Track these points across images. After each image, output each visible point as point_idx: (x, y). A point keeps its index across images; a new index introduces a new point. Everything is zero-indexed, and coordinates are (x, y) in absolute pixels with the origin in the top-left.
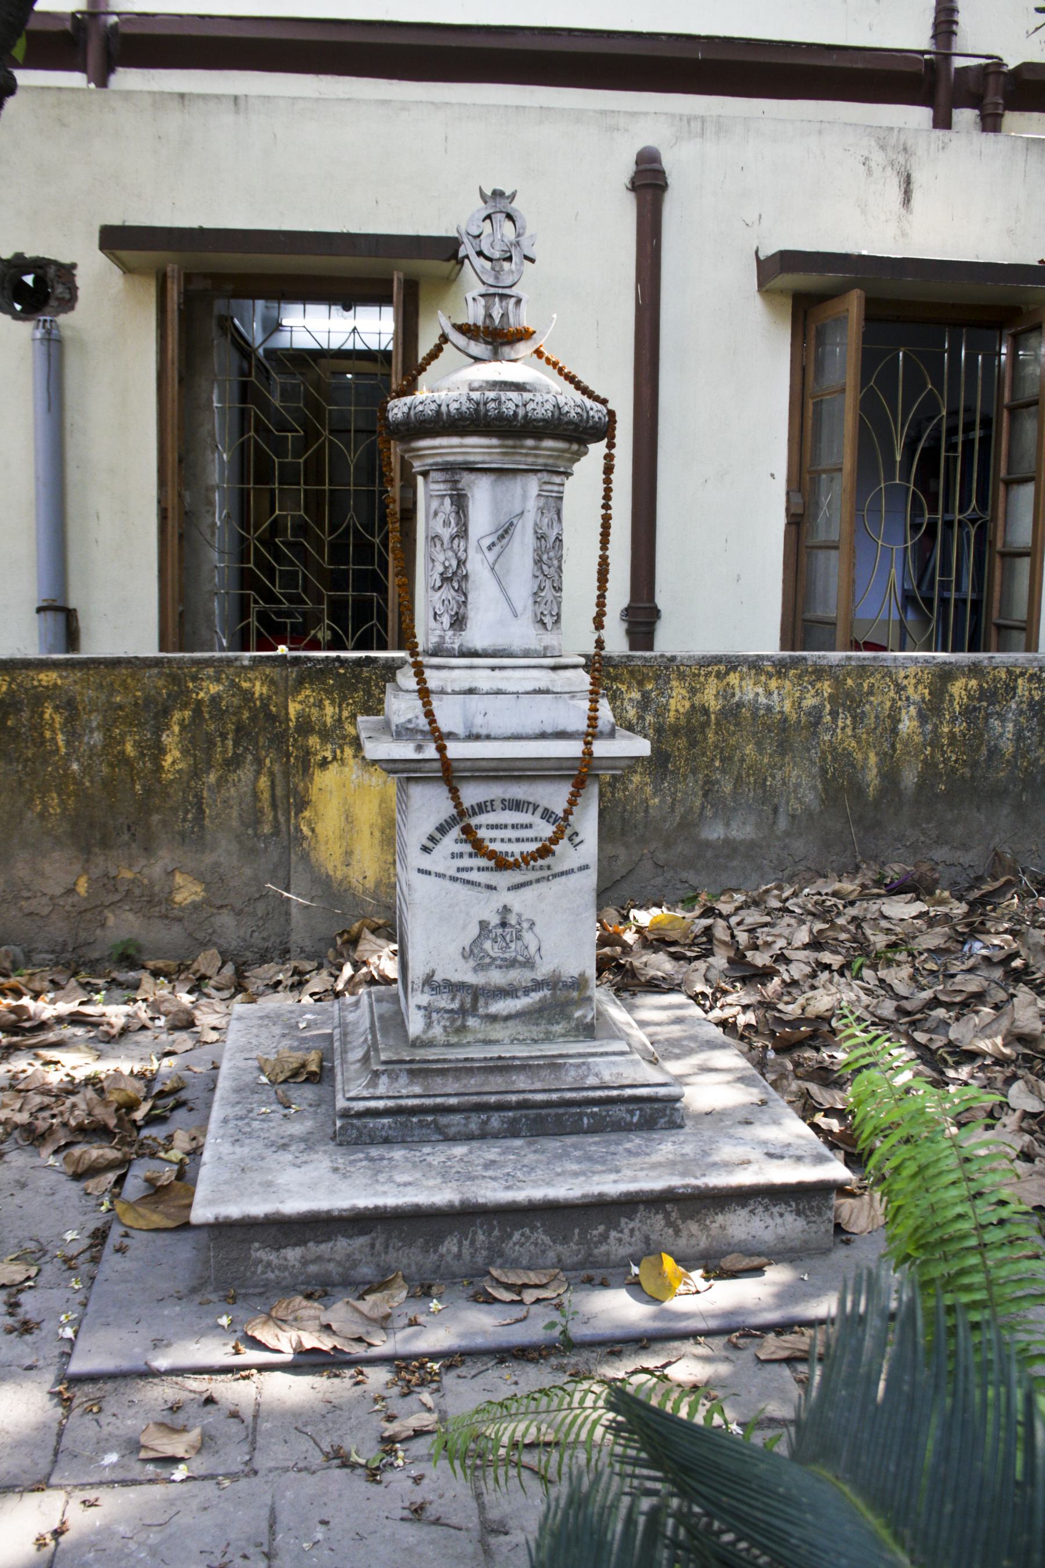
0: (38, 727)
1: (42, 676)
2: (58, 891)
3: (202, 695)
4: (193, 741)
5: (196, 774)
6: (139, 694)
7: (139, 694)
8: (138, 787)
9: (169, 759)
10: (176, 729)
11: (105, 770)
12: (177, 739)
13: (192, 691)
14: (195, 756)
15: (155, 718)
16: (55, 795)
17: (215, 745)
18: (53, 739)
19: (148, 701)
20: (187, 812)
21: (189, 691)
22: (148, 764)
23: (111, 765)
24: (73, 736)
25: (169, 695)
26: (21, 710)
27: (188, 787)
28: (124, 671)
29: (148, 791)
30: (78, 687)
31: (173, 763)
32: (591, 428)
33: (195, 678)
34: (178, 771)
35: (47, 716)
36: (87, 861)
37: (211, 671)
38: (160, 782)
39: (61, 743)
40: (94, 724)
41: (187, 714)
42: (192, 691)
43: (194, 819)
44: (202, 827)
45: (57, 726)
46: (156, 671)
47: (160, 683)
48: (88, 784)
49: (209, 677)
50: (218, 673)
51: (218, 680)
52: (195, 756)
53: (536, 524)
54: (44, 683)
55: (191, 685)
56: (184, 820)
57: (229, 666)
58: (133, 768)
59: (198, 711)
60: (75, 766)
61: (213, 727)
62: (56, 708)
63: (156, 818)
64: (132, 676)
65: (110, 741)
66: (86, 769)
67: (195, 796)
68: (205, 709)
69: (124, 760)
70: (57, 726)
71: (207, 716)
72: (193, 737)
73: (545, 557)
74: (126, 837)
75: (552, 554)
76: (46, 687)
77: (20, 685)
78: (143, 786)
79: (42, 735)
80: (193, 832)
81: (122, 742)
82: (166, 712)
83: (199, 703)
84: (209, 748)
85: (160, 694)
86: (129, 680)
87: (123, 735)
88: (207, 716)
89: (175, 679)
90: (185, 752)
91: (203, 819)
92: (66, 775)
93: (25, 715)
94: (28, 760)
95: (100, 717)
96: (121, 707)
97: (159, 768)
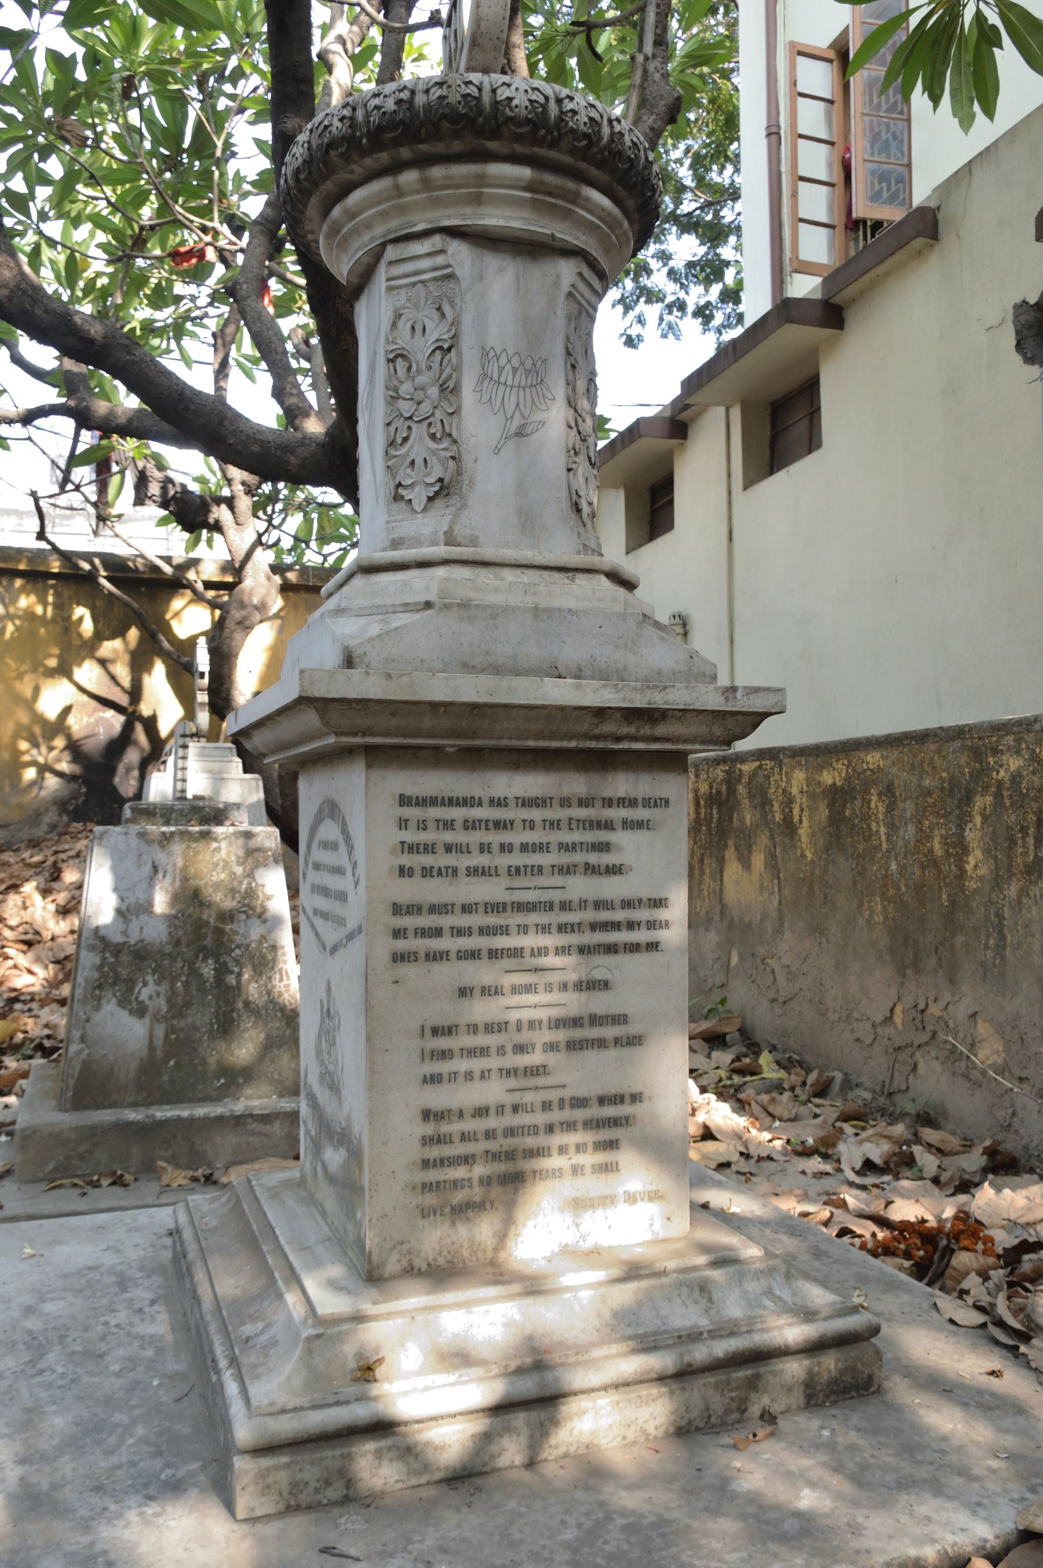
0: (866, 818)
1: (869, 758)
2: (879, 1018)
3: (1002, 773)
4: (994, 836)
5: (997, 884)
6: (944, 775)
7: (944, 775)
8: (944, 897)
9: (972, 861)
10: (978, 820)
11: (918, 872)
12: (979, 834)
13: (993, 769)
14: (996, 858)
15: (959, 806)
16: (878, 899)
17: (1016, 844)
18: (878, 831)
19: (954, 784)
20: (988, 937)
21: (990, 769)
22: (953, 867)
23: (923, 867)
24: (893, 828)
25: (971, 774)
26: (855, 798)
27: (990, 901)
28: (932, 747)
29: (953, 902)
30: (895, 769)
31: (976, 866)
32: (380, 128)
33: (995, 752)
34: (981, 879)
35: (873, 805)
36: (902, 985)
37: (1010, 740)
38: (963, 892)
39: (883, 837)
40: (908, 814)
41: (989, 799)
42: (993, 769)
43: (997, 946)
44: (1003, 959)
45: (881, 816)
46: (958, 744)
47: (963, 759)
48: (903, 889)
49: (1009, 750)
50: (1018, 741)
51: (1018, 752)
52: (996, 858)
53: (387, 339)
54: (871, 766)
55: (991, 760)
56: (986, 947)
57: (1029, 731)
58: (940, 871)
59: (998, 796)
60: (894, 867)
61: (1013, 818)
62: (880, 794)
63: (960, 939)
64: (938, 751)
65: (924, 836)
66: (903, 868)
67: (997, 915)
68: (1005, 793)
69: (932, 862)
70: (881, 816)
71: (1007, 802)
72: (994, 832)
73: (405, 389)
74: (933, 961)
75: (421, 380)
76: (872, 770)
77: (854, 770)
78: (949, 896)
79: (869, 825)
80: (994, 966)
81: (930, 838)
82: (968, 799)
83: (1000, 783)
84: (1010, 848)
85: (963, 774)
86: (936, 758)
87: (931, 828)
88: (1007, 802)
89: (977, 754)
90: (987, 852)
91: (1004, 948)
92: (886, 877)
93: (858, 803)
94: (860, 856)
95: (913, 806)
96: (929, 793)
97: (962, 874)
